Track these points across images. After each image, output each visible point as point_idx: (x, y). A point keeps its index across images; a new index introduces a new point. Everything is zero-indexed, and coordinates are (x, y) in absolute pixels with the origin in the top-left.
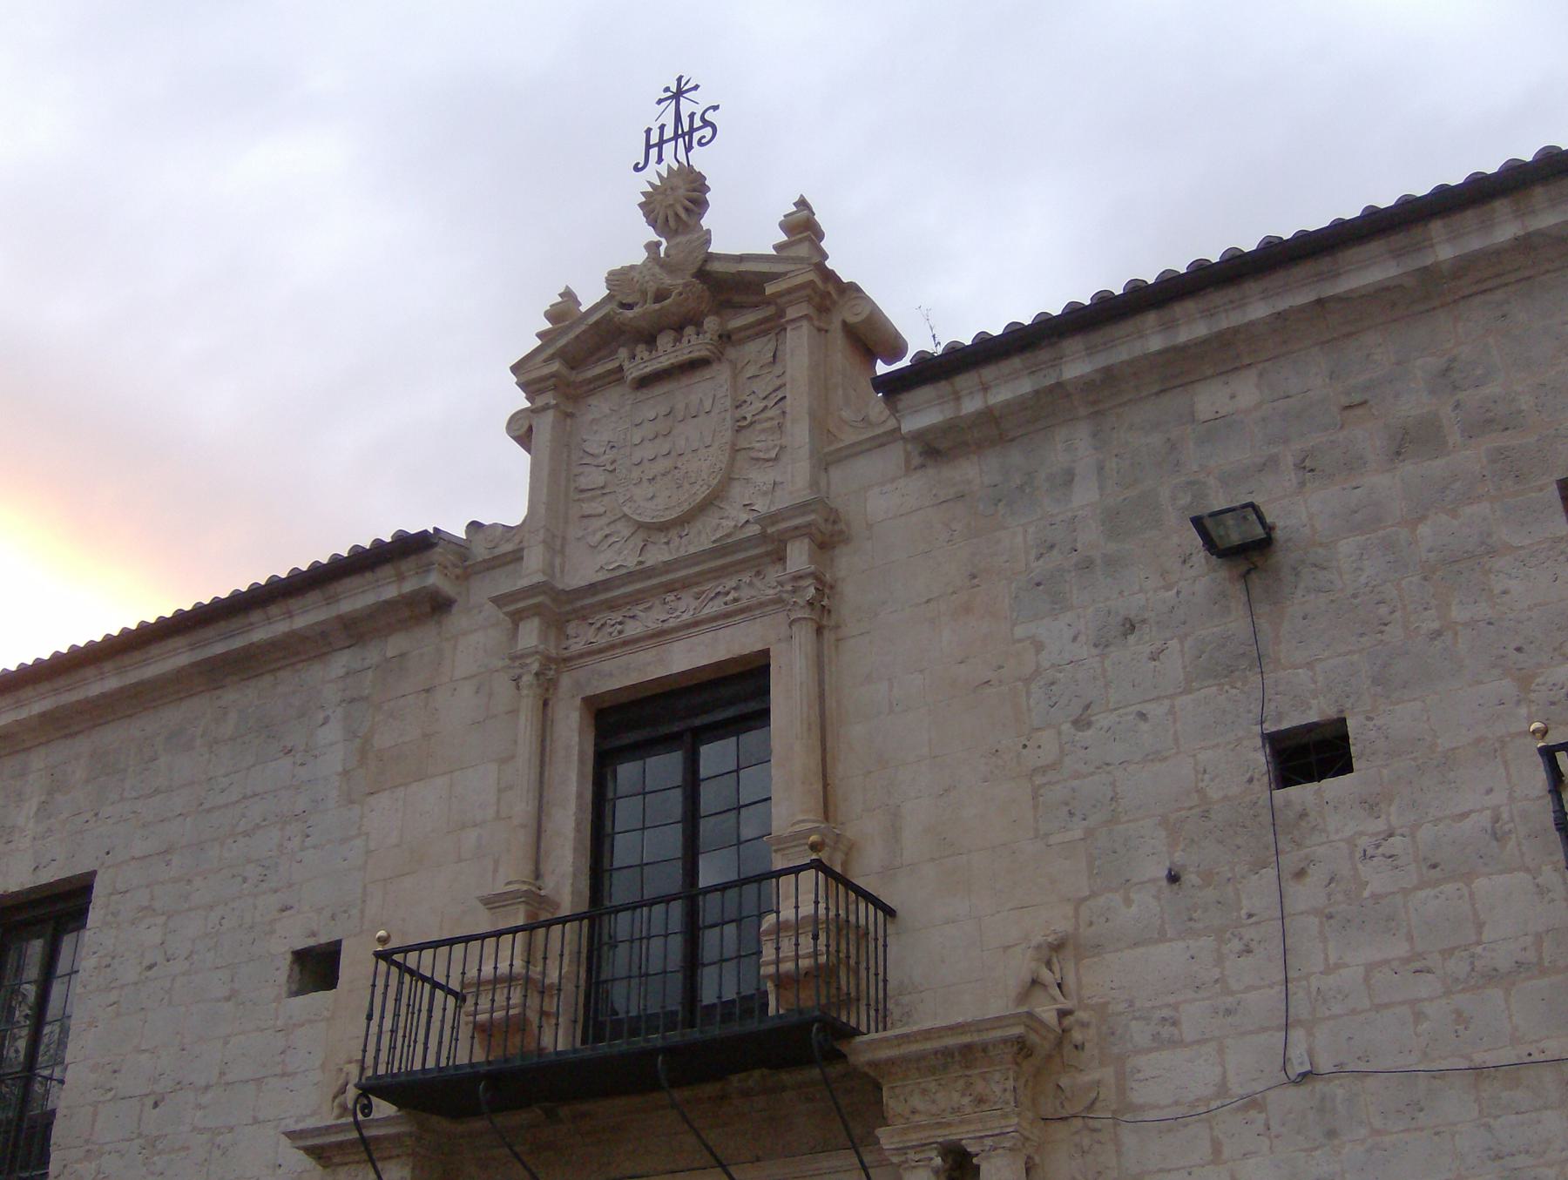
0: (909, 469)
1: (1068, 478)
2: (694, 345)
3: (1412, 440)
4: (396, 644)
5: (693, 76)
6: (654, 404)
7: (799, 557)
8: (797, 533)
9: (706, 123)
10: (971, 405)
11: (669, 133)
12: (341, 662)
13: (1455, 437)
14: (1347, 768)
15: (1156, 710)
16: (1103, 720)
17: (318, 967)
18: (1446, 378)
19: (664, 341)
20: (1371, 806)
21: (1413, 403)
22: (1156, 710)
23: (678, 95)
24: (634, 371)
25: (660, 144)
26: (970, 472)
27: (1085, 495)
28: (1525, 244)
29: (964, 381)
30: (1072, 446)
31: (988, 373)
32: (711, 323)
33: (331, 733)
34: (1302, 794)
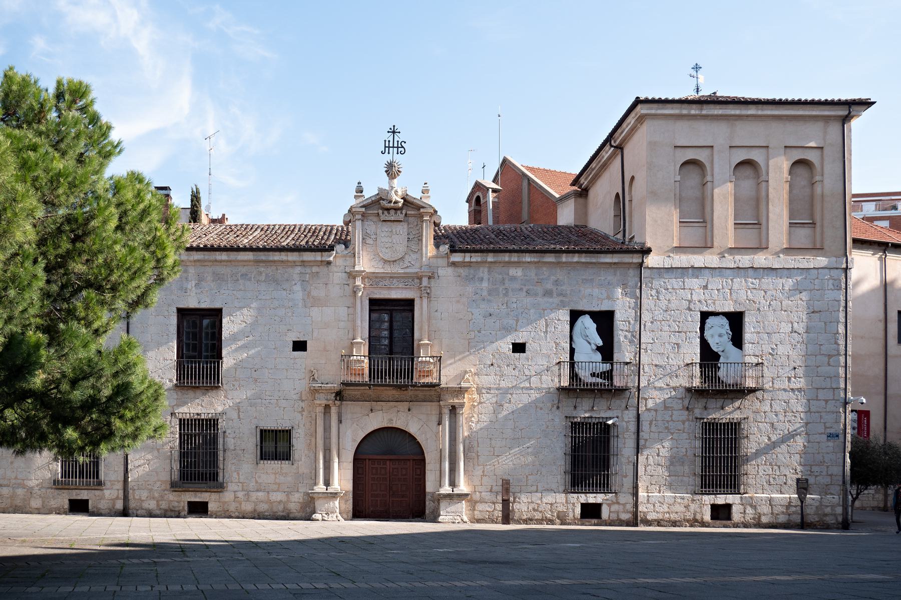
0: (448, 266)
1: (482, 280)
2: (401, 217)
3: (548, 293)
4: (315, 269)
5: (398, 128)
6: (386, 227)
7: (425, 282)
8: (426, 276)
9: (402, 147)
10: (467, 259)
11: (391, 145)
12: (298, 269)
13: (555, 295)
14: (524, 352)
15: (493, 333)
16: (483, 332)
17: (299, 346)
18: (557, 283)
19: (392, 212)
20: (528, 359)
21: (549, 286)
22: (493, 333)
23: (394, 132)
24: (383, 217)
25: (389, 147)
26: (461, 270)
27: (485, 284)
28: (577, 262)
29: (468, 255)
30: (483, 272)
31: (473, 254)
32: (404, 212)
33: (298, 288)
34: (517, 355)
